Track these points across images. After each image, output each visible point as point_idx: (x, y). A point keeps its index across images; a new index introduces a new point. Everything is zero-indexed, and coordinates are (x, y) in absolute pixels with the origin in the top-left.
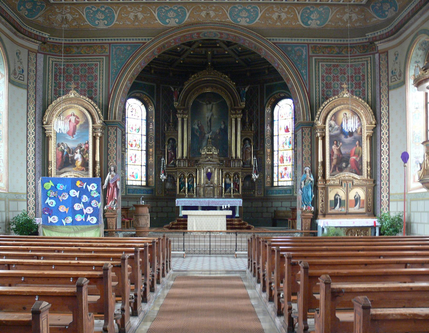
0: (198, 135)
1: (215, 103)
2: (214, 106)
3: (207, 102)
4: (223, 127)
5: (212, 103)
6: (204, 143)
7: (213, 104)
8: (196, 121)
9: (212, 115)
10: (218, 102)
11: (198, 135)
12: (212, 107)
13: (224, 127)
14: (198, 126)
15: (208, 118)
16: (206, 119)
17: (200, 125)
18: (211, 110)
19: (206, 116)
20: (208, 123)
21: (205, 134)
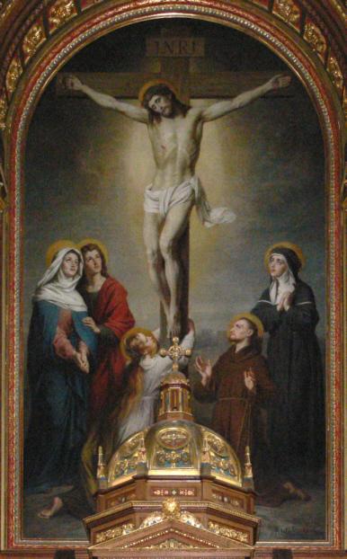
0: (85, 365)
1: (217, 107)
2: (209, 130)
3: (160, 104)
4: (281, 293)
5: (197, 105)
6: (134, 425)
7: (200, 119)
8: (64, 254)
9: (197, 201)
10: (244, 98)
11: (85, 365)
12: (196, 139)
13: (293, 299)
14: (81, 287)
15: (161, 224)
16: (149, 230)
17: (99, 282)
18: (190, 166)
19: (150, 208)
20: (160, 265)
21: (138, 353)
